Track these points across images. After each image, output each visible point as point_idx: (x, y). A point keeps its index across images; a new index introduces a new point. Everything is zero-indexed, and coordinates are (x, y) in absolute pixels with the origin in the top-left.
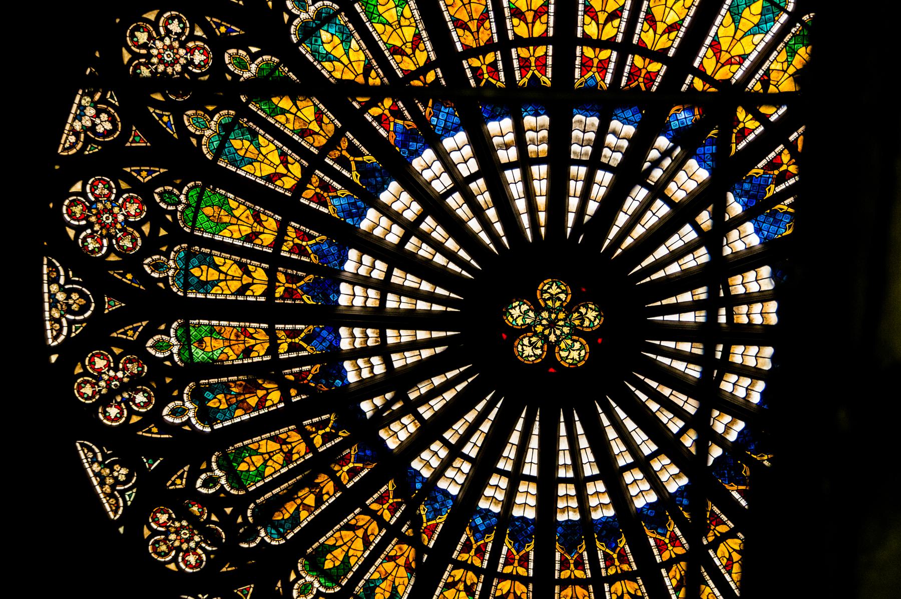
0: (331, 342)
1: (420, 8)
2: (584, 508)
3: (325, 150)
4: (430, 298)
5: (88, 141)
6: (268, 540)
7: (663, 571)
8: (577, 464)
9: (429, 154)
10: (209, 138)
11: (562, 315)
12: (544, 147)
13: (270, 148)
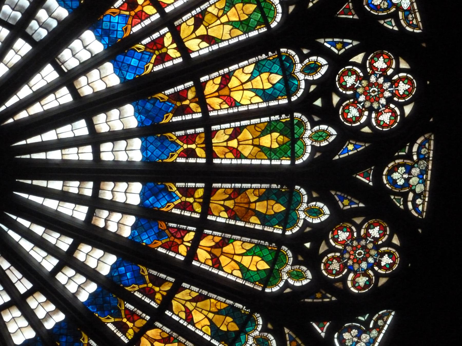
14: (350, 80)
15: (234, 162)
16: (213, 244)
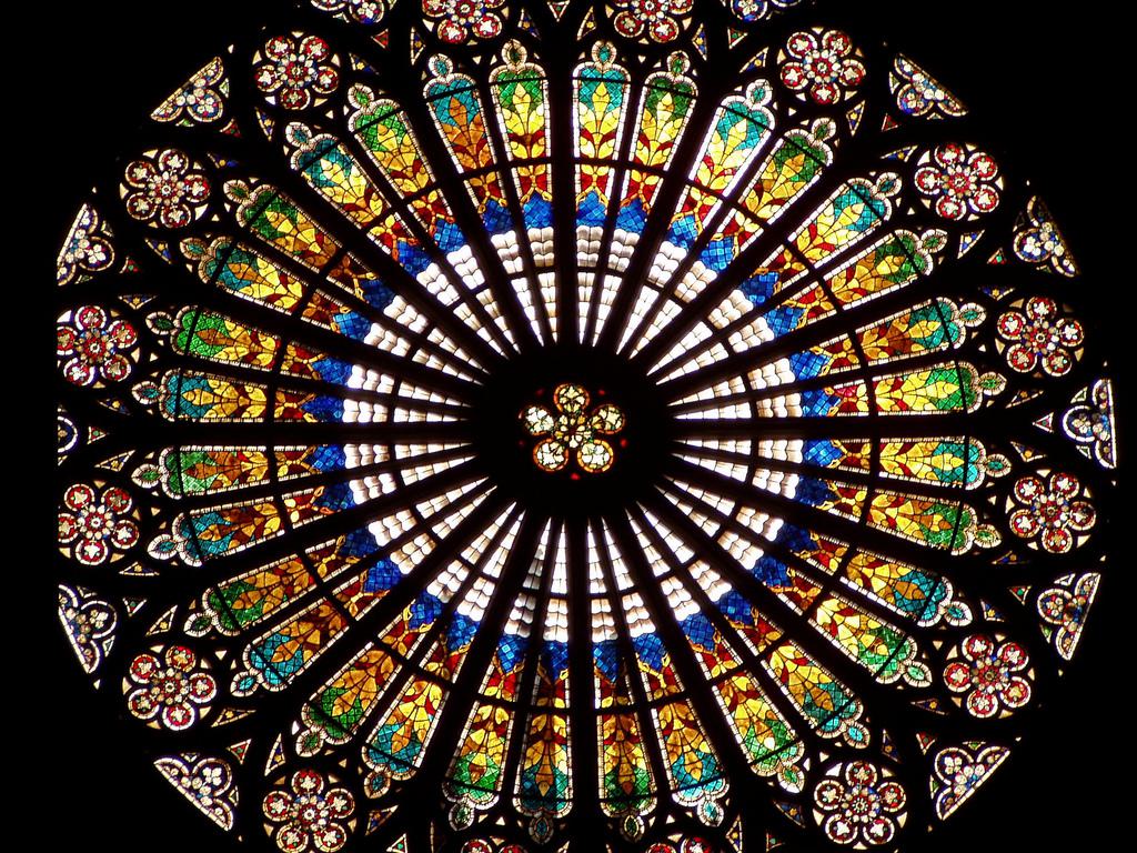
0: (336, 461)
3: (325, 270)
4: (441, 409)
5: (79, 271)
6: (267, 687)
7: (714, 688)
8: (609, 578)
9: (433, 269)
10: (206, 263)
11: (582, 420)
12: (551, 256)
13: (269, 271)
14: (930, 181)
16: (889, 388)
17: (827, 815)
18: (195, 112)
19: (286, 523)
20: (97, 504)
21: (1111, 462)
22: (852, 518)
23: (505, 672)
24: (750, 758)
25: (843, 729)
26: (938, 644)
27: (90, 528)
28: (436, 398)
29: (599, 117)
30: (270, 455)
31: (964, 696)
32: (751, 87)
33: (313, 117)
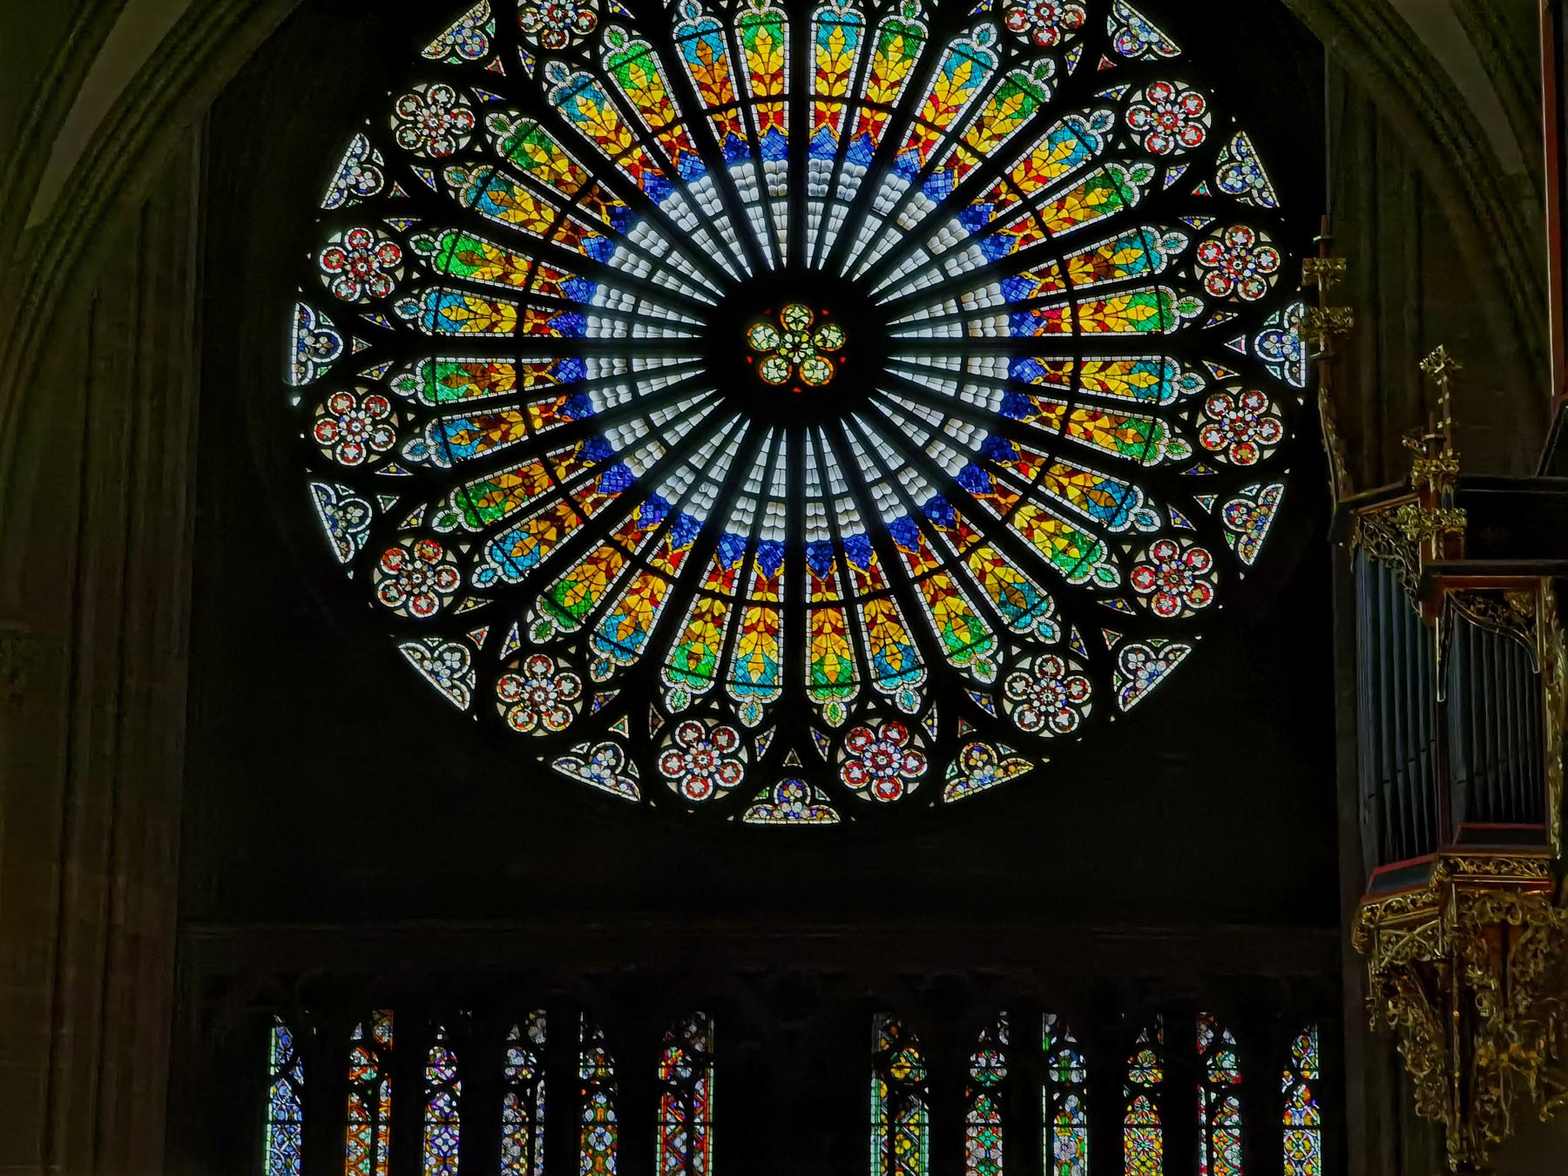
1: (667, 75)
2: (834, 528)
3: (576, 197)
4: (677, 326)
5: (351, 196)
6: (505, 578)
7: (917, 587)
8: (825, 484)
9: (675, 196)
11: (805, 338)
13: (524, 196)
14: (1140, 118)
15: (1073, 229)
17: (1016, 704)
18: (463, 50)
19: (530, 430)
20: (358, 410)
21: (1299, 381)
22: (1051, 431)
23: (724, 568)
24: (946, 651)
25: (1034, 625)
26: (1127, 548)
27: (350, 432)
28: (672, 316)
29: (835, 58)
30: (519, 370)
31: (1149, 597)
32: (977, 30)
33: (570, 56)
